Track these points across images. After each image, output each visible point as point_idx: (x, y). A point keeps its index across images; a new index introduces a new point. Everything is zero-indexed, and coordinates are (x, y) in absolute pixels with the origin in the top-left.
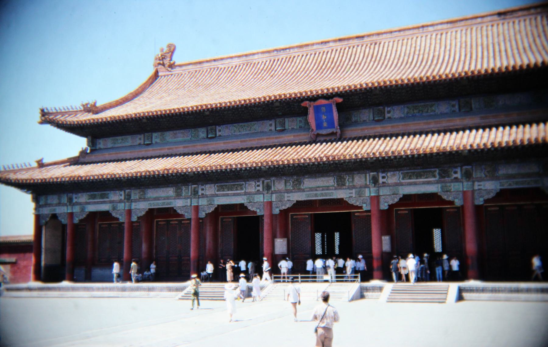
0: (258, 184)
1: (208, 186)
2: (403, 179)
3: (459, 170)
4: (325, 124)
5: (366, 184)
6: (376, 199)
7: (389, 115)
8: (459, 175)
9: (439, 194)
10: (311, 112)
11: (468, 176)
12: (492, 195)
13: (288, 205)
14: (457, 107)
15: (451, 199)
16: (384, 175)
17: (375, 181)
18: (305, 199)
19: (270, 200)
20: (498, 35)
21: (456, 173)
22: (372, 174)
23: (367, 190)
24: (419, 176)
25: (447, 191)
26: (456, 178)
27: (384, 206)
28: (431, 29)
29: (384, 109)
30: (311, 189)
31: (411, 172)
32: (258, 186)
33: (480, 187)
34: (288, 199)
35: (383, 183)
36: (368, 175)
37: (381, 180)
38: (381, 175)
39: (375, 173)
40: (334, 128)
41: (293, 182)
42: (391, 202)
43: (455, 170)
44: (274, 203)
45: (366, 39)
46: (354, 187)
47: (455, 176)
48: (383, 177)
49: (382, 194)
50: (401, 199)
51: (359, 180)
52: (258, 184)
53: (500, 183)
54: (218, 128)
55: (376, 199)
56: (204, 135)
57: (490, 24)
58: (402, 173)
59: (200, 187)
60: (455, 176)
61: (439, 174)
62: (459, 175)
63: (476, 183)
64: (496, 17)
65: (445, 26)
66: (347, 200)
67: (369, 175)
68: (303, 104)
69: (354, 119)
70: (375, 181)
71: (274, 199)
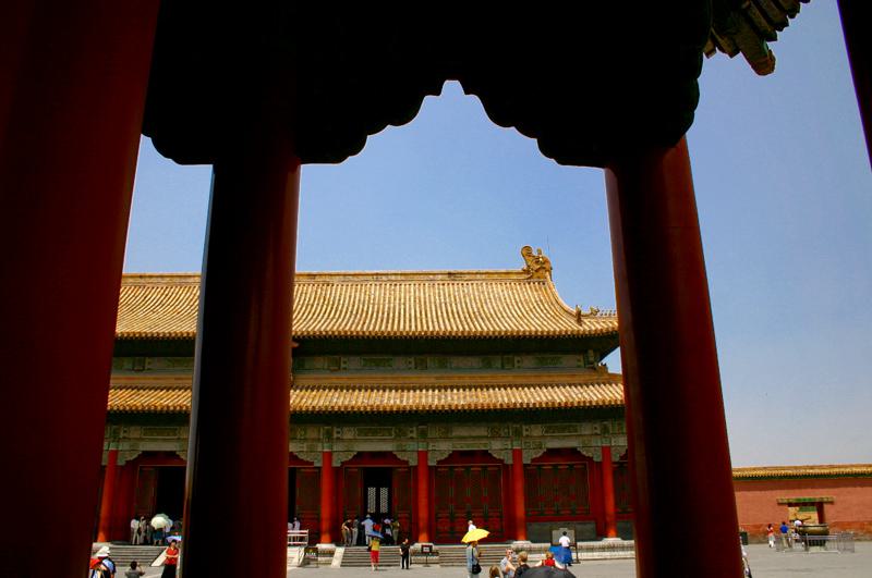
1: (132, 428)
3: (415, 429)
5: (319, 439)
6: (328, 456)
8: (414, 435)
11: (423, 434)
12: (446, 456)
14: (413, 363)
17: (329, 435)
20: (449, 295)
21: (412, 432)
23: (320, 445)
24: (375, 433)
26: (412, 438)
27: (336, 463)
28: (384, 278)
35: (338, 438)
37: (335, 436)
38: (335, 430)
42: (344, 459)
45: (318, 279)
46: (305, 439)
47: (411, 435)
48: (338, 433)
50: (355, 456)
51: (312, 433)
54: (148, 360)
55: (328, 456)
56: (130, 367)
57: (441, 282)
59: (123, 428)
60: (411, 435)
62: (414, 435)
63: (431, 444)
64: (446, 277)
65: (399, 278)
69: (307, 366)
70: (329, 435)
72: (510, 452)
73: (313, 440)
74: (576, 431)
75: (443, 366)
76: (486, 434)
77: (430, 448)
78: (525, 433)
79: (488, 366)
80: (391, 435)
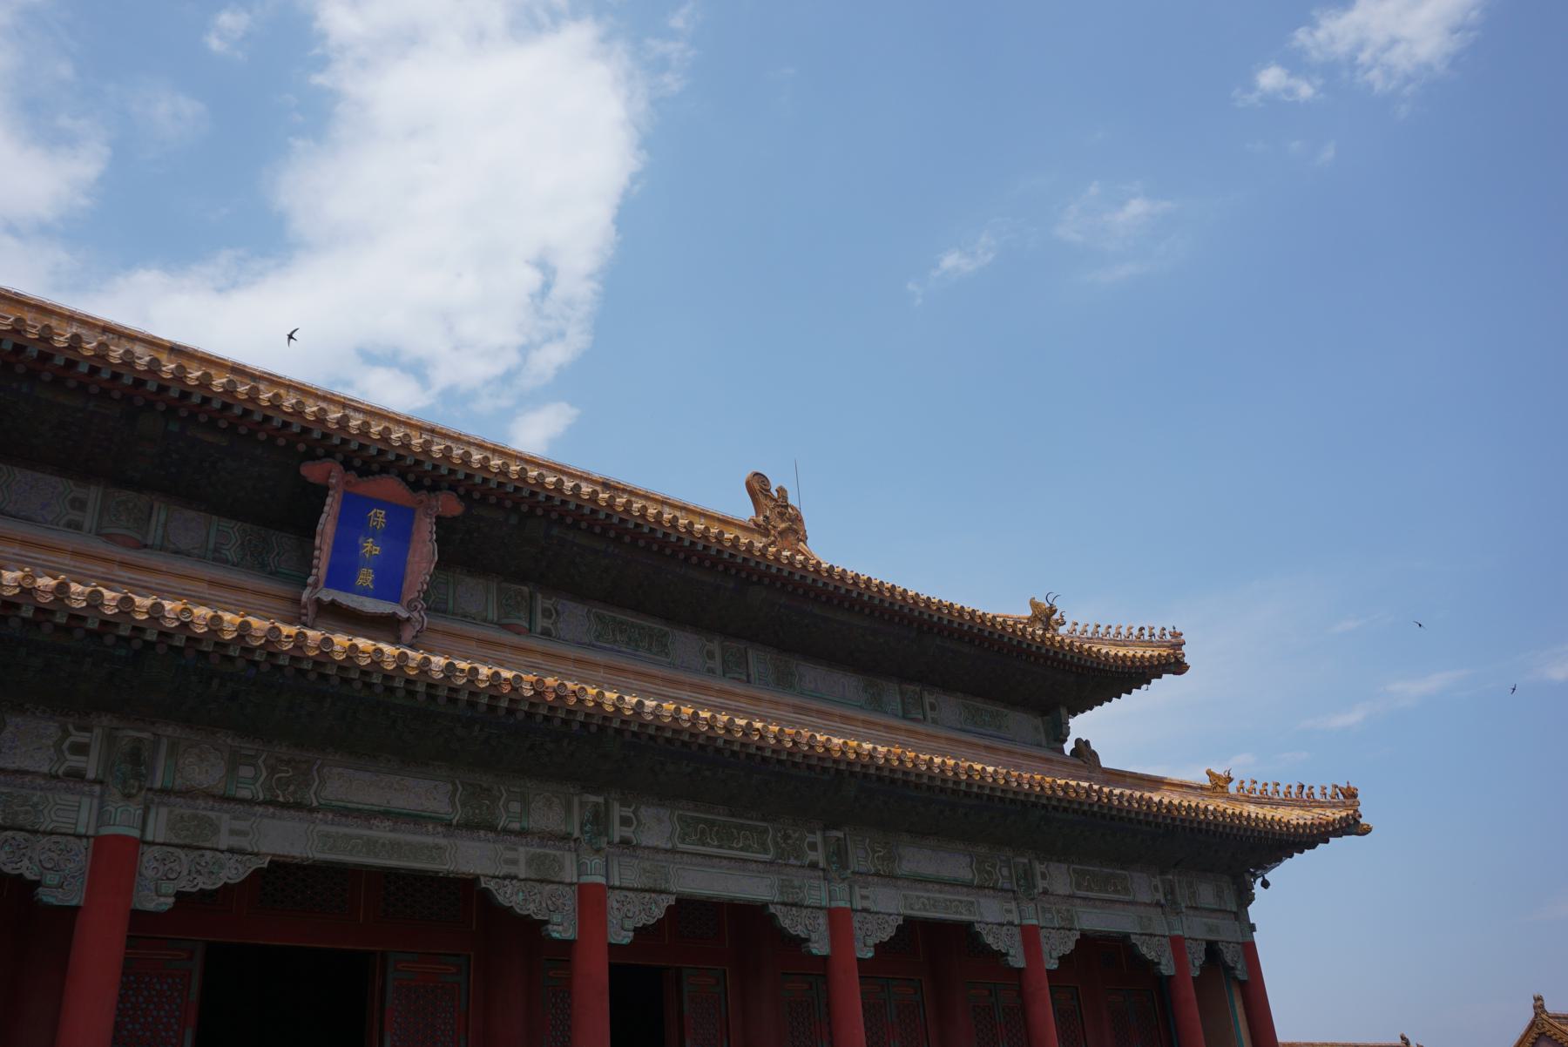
0: (80, 737)
2: (683, 841)
4: (366, 577)
6: (591, 900)
7: (547, 623)
8: (819, 856)
9: (772, 909)
10: (332, 506)
13: (233, 872)
15: (800, 931)
16: (628, 812)
18: (319, 856)
19: (136, 833)
21: (813, 846)
22: (593, 798)
25: (794, 905)
26: (814, 866)
29: (532, 597)
30: (345, 812)
31: (705, 821)
32: (81, 749)
33: (866, 904)
34: (236, 842)
35: (625, 842)
36: (576, 800)
38: (617, 811)
39: (601, 800)
40: (396, 598)
41: (272, 770)
42: (643, 920)
43: (810, 838)
44: (149, 855)
48: (625, 822)
49: (617, 883)
52: (80, 737)
53: (906, 897)
58: (680, 818)
60: (812, 856)
61: (776, 843)
62: (819, 856)
66: (492, 885)
67: (582, 805)
68: (312, 471)
71: (158, 829)
72: (1016, 931)
73: (547, 837)
74: (1126, 890)
75: (784, 681)
76: (965, 874)
77: (858, 904)
78: (1041, 884)
79: (876, 703)
80: (766, 851)
